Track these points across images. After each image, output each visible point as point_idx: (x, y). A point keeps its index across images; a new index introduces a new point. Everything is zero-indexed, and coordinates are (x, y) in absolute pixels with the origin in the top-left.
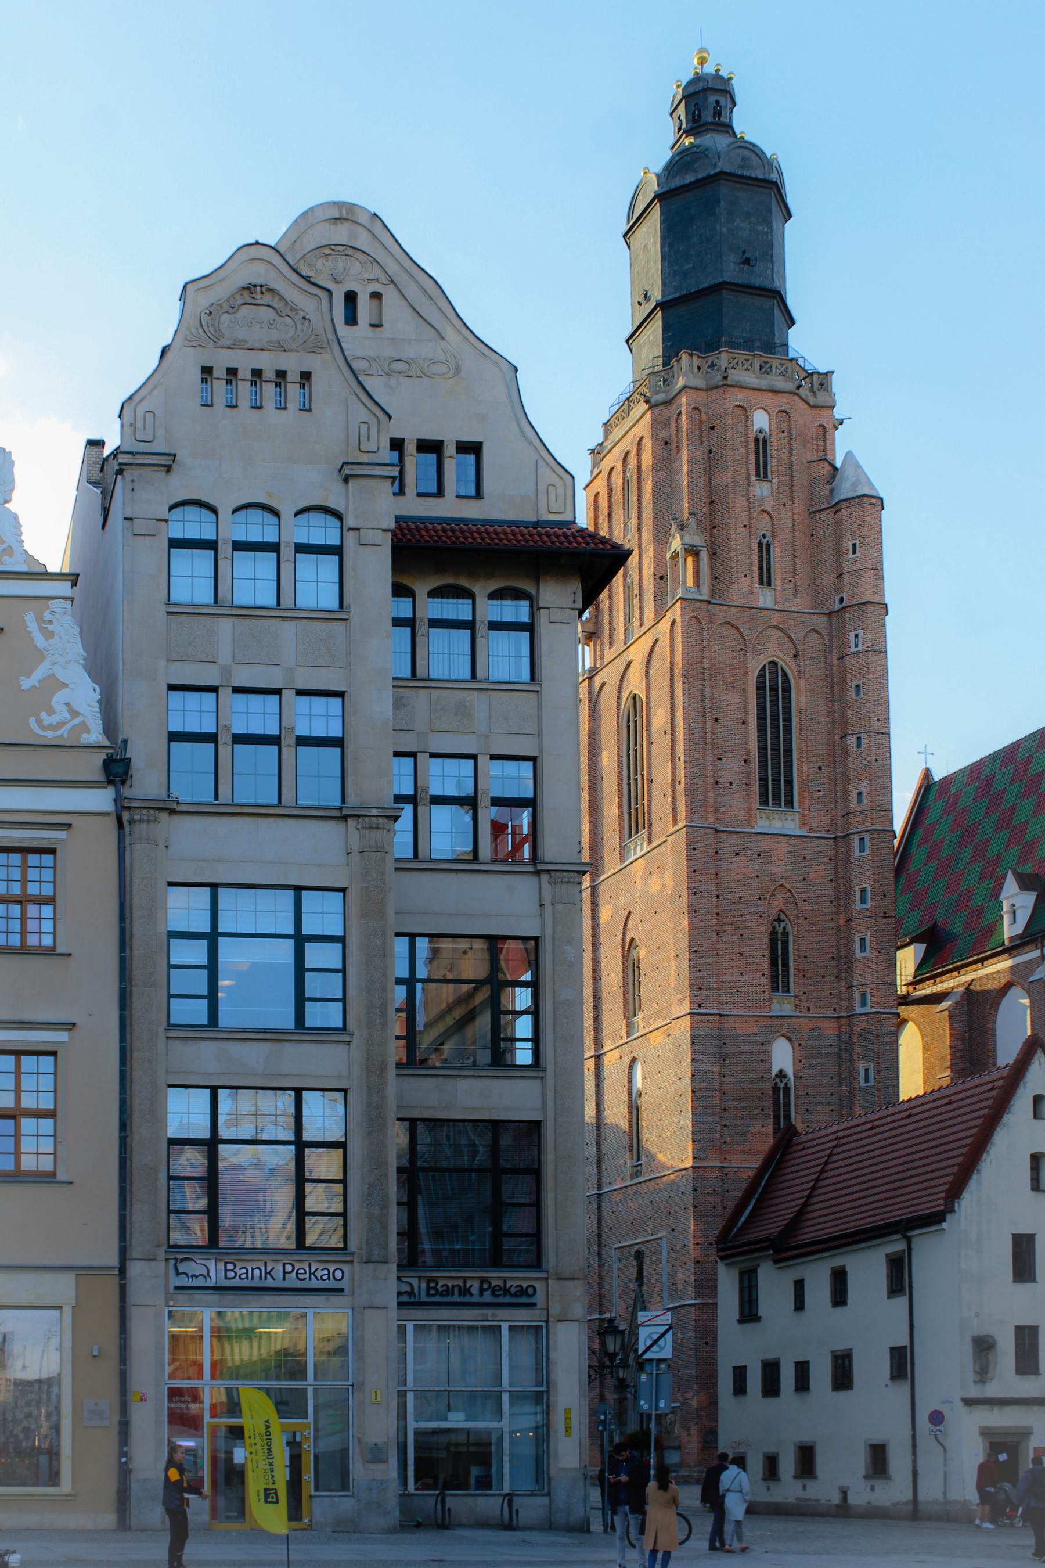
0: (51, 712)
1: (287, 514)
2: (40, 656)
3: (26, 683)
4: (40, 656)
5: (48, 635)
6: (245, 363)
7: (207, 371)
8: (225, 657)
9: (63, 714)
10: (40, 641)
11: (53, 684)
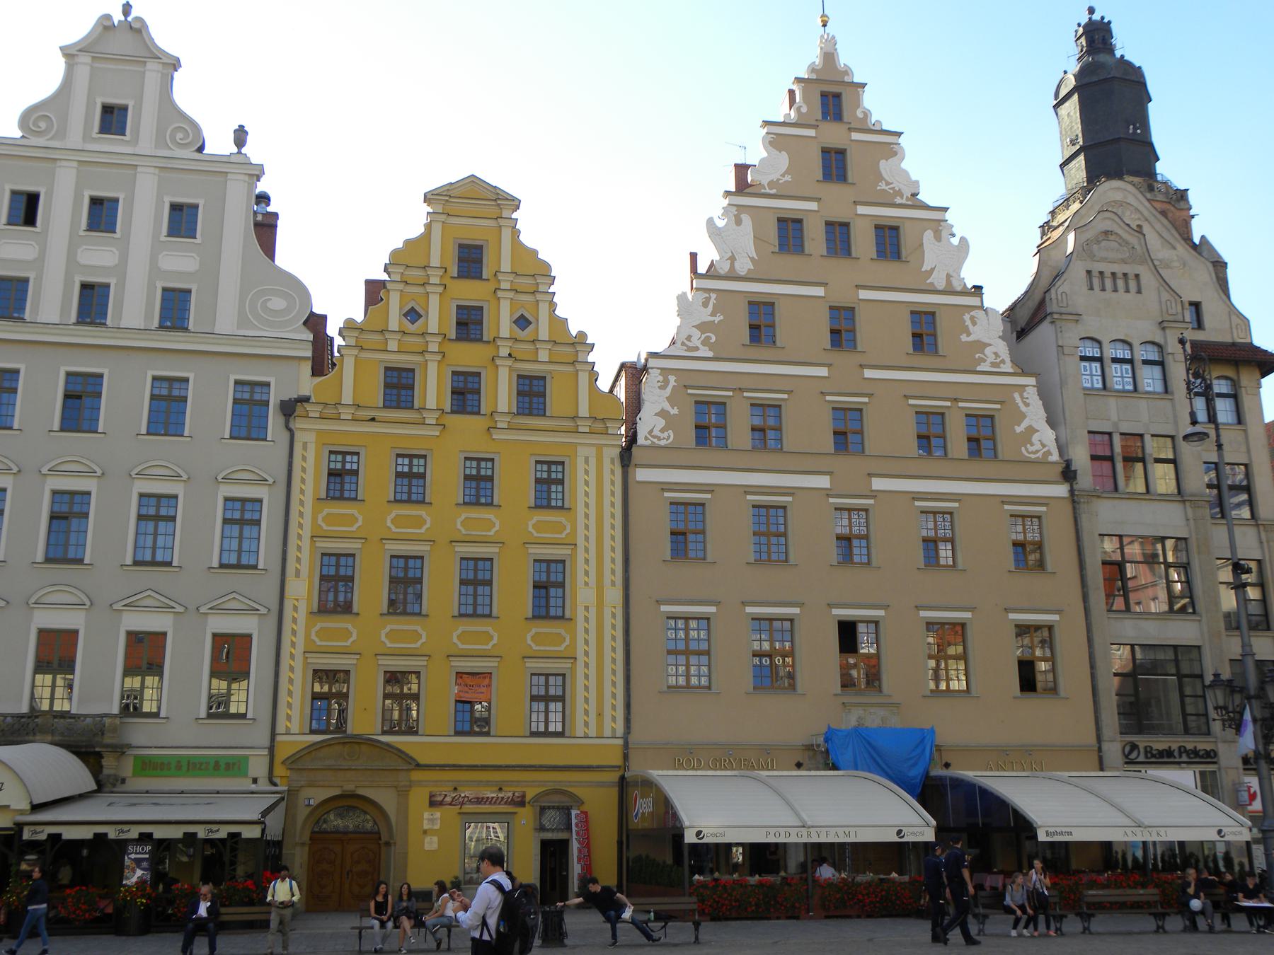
0: (1032, 445)
1: (1136, 343)
2: (1023, 416)
3: (1018, 429)
4: (1023, 416)
5: (1027, 405)
6: (1108, 268)
7: (1089, 272)
8: (1114, 418)
9: (1037, 446)
10: (1023, 408)
11: (1031, 430)
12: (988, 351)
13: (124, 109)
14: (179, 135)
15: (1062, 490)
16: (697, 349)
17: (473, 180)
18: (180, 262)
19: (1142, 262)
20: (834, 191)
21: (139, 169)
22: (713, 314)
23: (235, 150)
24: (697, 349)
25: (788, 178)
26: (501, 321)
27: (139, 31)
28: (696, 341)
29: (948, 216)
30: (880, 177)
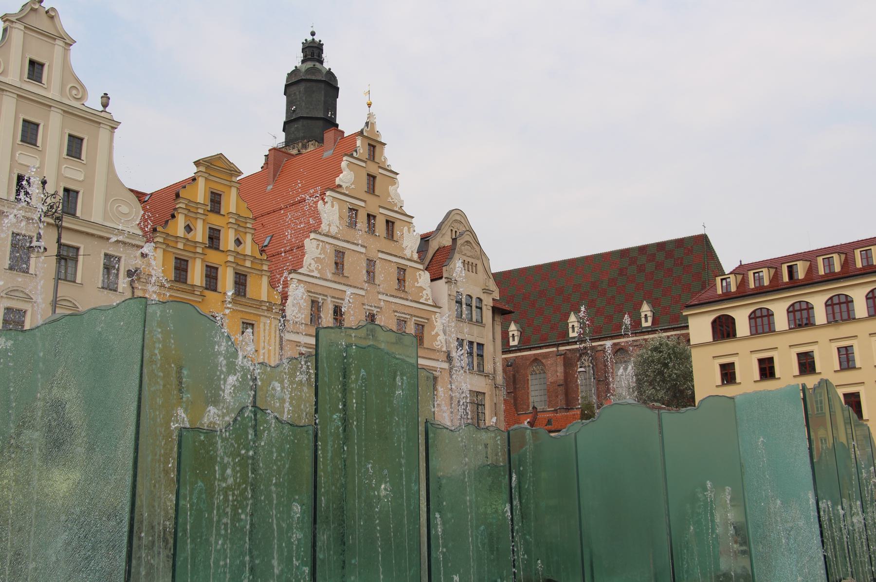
9: (439, 343)
11: (437, 335)
12: (424, 292)
13: (42, 65)
14: (74, 92)
15: (446, 366)
16: (313, 271)
17: (220, 157)
18: (73, 174)
19: (478, 259)
20: (369, 198)
21: (52, 109)
22: (320, 254)
23: (101, 108)
24: (313, 271)
25: (353, 186)
26: (228, 240)
27: (52, 17)
28: (313, 267)
29: (413, 220)
30: (389, 195)
